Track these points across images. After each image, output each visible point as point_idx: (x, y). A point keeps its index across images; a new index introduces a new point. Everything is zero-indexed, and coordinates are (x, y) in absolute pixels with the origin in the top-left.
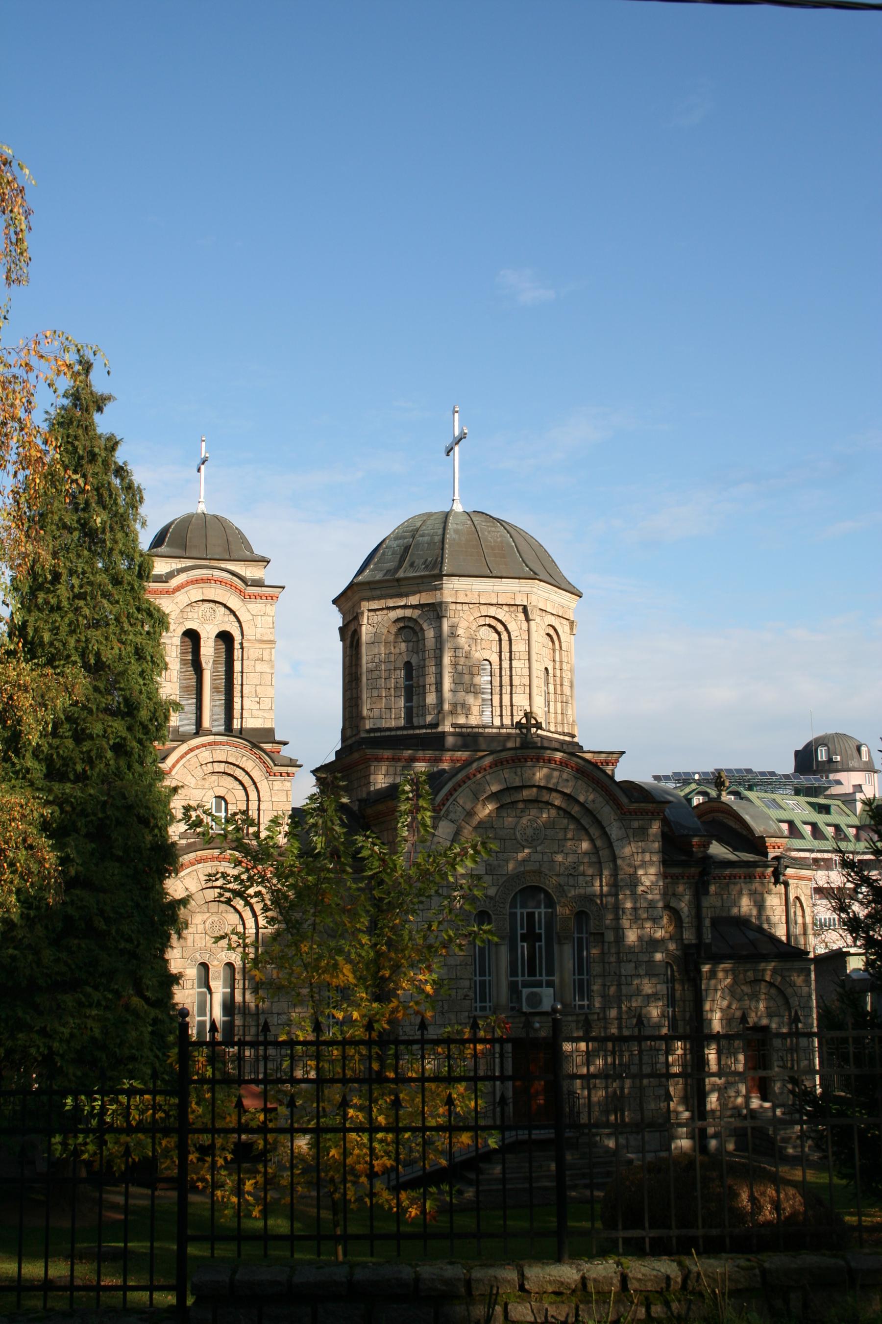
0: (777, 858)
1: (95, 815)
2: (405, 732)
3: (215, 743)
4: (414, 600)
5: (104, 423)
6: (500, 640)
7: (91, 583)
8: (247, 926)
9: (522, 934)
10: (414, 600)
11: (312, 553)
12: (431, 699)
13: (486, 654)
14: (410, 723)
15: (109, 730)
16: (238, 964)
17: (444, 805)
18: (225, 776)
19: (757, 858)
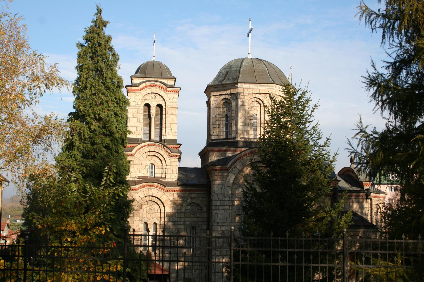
0: (367, 189)
1: (98, 171)
2: (225, 141)
3: (150, 145)
4: (228, 92)
5: (107, 31)
6: (260, 107)
7: (98, 89)
10: (228, 92)
11: (195, 73)
12: (234, 129)
13: (255, 112)
14: (227, 138)
15: (103, 141)
16: (158, 224)
17: (231, 168)
18: (154, 157)
19: (358, 189)
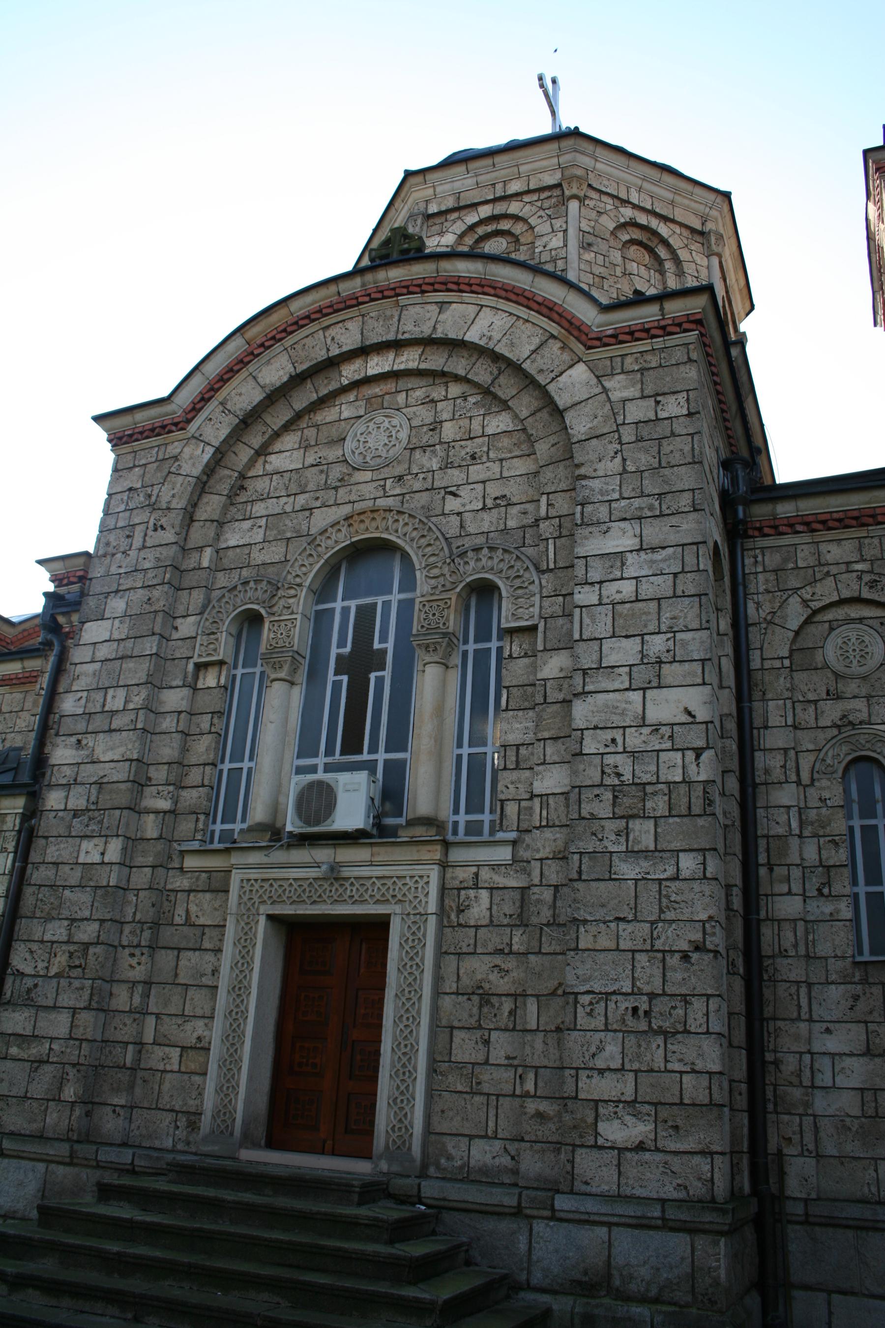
9: (339, 657)
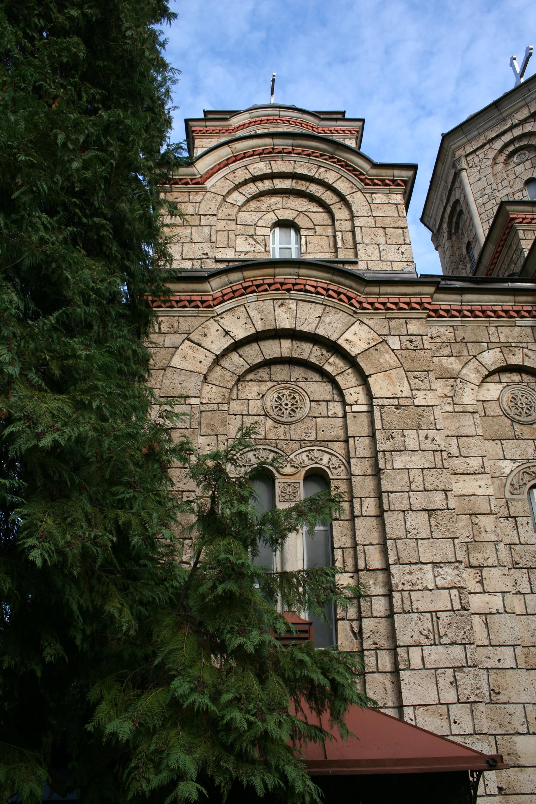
8: (349, 399)
